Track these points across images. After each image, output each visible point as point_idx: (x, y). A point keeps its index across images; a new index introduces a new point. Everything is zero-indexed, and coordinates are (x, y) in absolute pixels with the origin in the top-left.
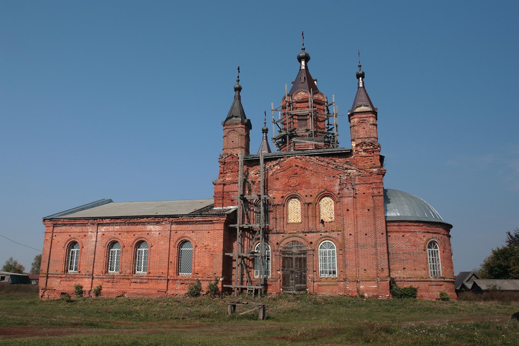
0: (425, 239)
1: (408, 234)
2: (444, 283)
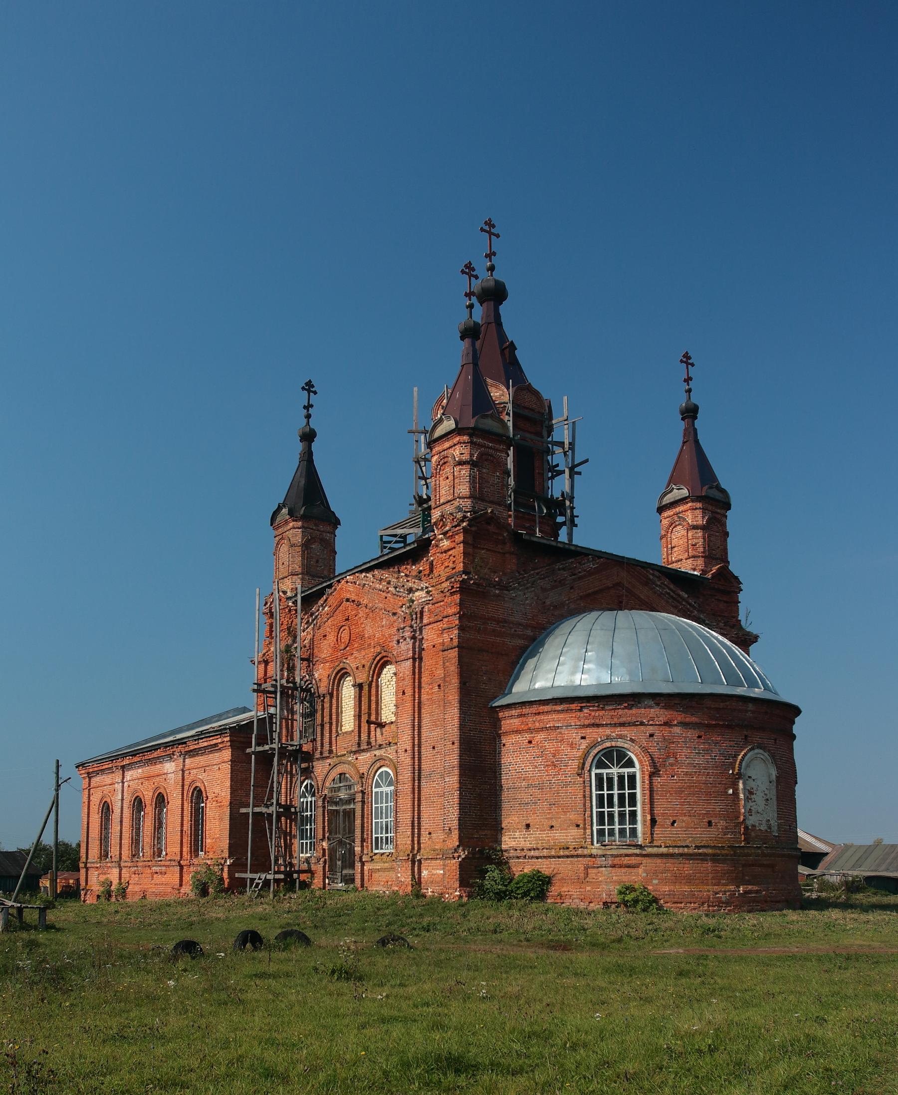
0: (584, 744)
1: (540, 736)
2: (645, 861)
